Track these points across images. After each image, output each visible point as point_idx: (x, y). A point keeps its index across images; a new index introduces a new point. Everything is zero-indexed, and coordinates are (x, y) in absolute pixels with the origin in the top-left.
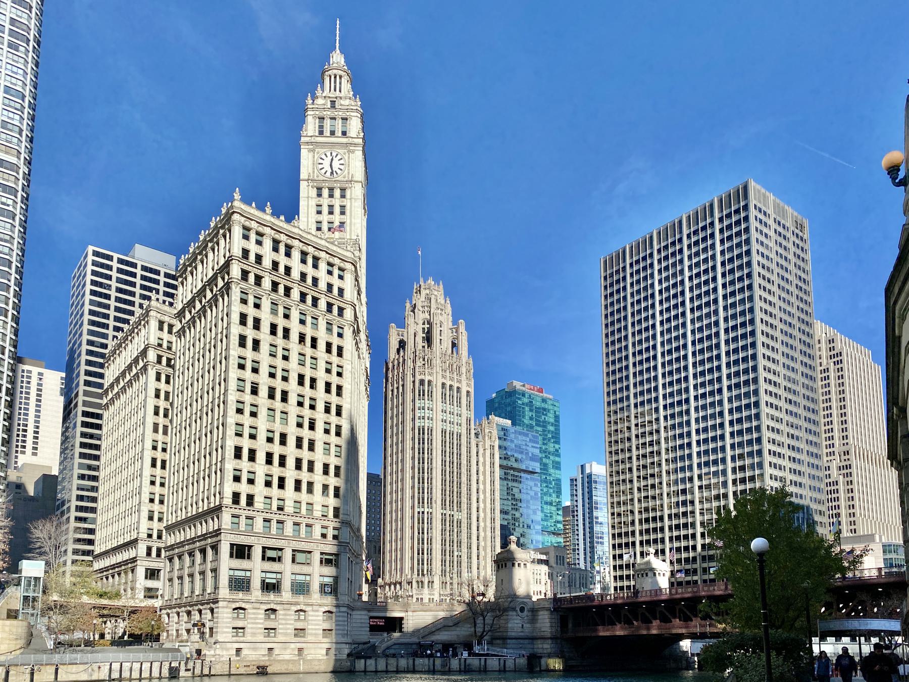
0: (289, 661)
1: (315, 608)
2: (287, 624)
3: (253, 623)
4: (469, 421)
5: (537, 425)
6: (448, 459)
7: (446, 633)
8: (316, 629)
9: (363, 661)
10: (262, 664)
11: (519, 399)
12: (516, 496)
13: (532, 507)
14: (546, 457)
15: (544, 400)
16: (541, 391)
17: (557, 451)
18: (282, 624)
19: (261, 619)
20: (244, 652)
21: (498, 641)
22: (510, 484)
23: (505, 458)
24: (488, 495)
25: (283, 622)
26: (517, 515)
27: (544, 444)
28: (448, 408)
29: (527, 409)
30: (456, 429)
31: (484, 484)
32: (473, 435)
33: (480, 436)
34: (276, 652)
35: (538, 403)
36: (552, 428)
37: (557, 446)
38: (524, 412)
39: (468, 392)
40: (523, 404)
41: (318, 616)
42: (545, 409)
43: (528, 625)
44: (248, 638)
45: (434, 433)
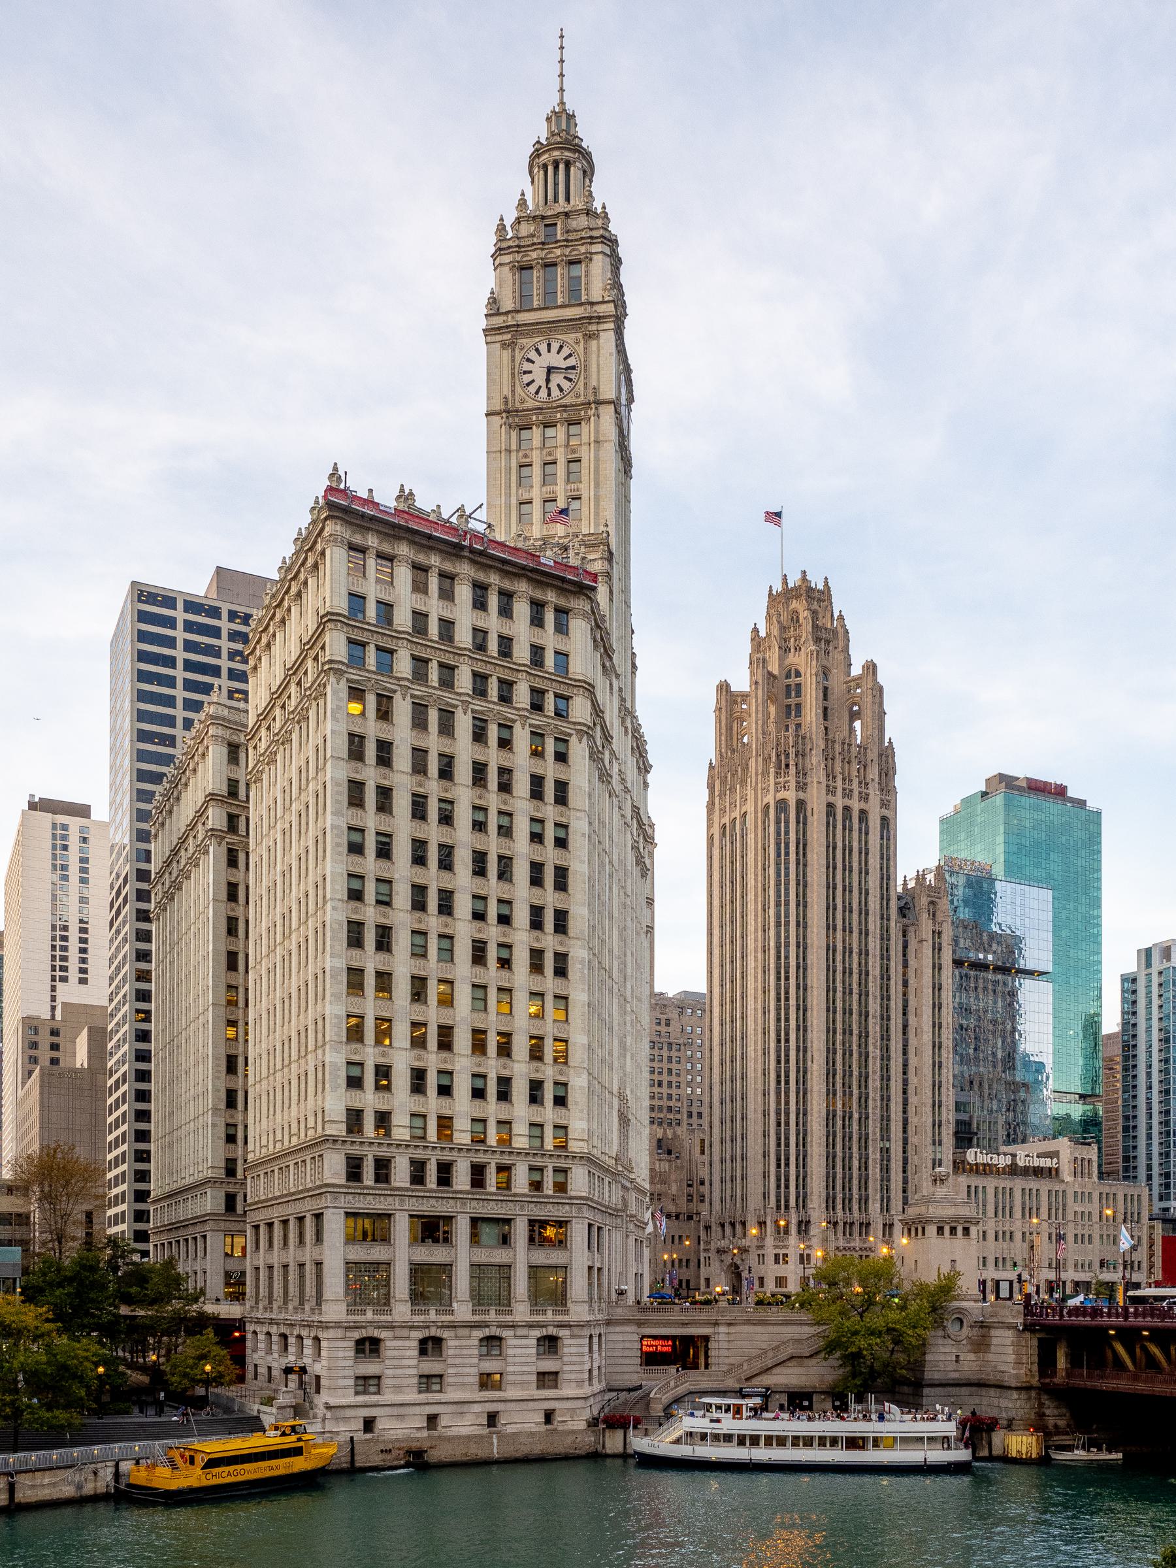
0: (468, 1438)
1: (520, 1332)
2: (464, 1365)
3: (396, 1367)
7: (799, 1370)
8: (523, 1373)
9: (620, 1433)
10: (415, 1445)
18: (455, 1366)
19: (410, 1358)
20: (381, 1425)
21: (906, 1389)
25: (457, 1361)
34: (444, 1421)
41: (527, 1347)
43: (972, 1357)
44: (387, 1397)
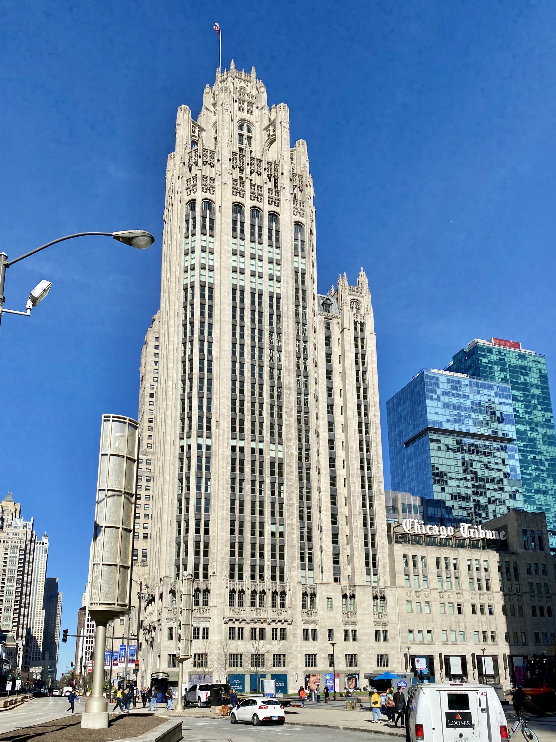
4: (299, 276)
5: (513, 388)
6: (248, 341)
11: (484, 356)
12: (479, 473)
13: (507, 489)
14: (532, 430)
15: (522, 357)
16: (516, 345)
17: (549, 421)
22: (467, 457)
23: (456, 421)
24: (352, 412)
26: (483, 501)
27: (527, 412)
28: (248, 247)
29: (496, 368)
30: (267, 287)
31: (343, 392)
32: (313, 304)
33: (334, 309)
35: (512, 360)
36: (537, 392)
37: (548, 415)
38: (492, 373)
39: (298, 225)
40: (490, 362)
42: (524, 368)
45: (216, 294)
